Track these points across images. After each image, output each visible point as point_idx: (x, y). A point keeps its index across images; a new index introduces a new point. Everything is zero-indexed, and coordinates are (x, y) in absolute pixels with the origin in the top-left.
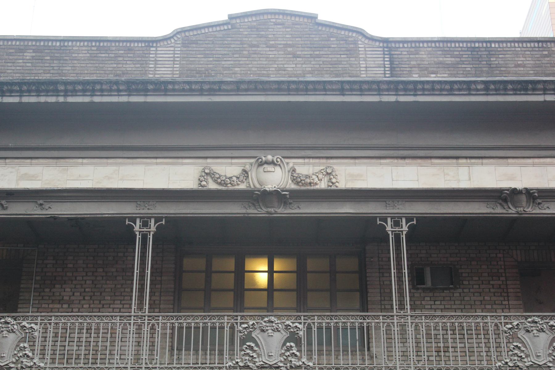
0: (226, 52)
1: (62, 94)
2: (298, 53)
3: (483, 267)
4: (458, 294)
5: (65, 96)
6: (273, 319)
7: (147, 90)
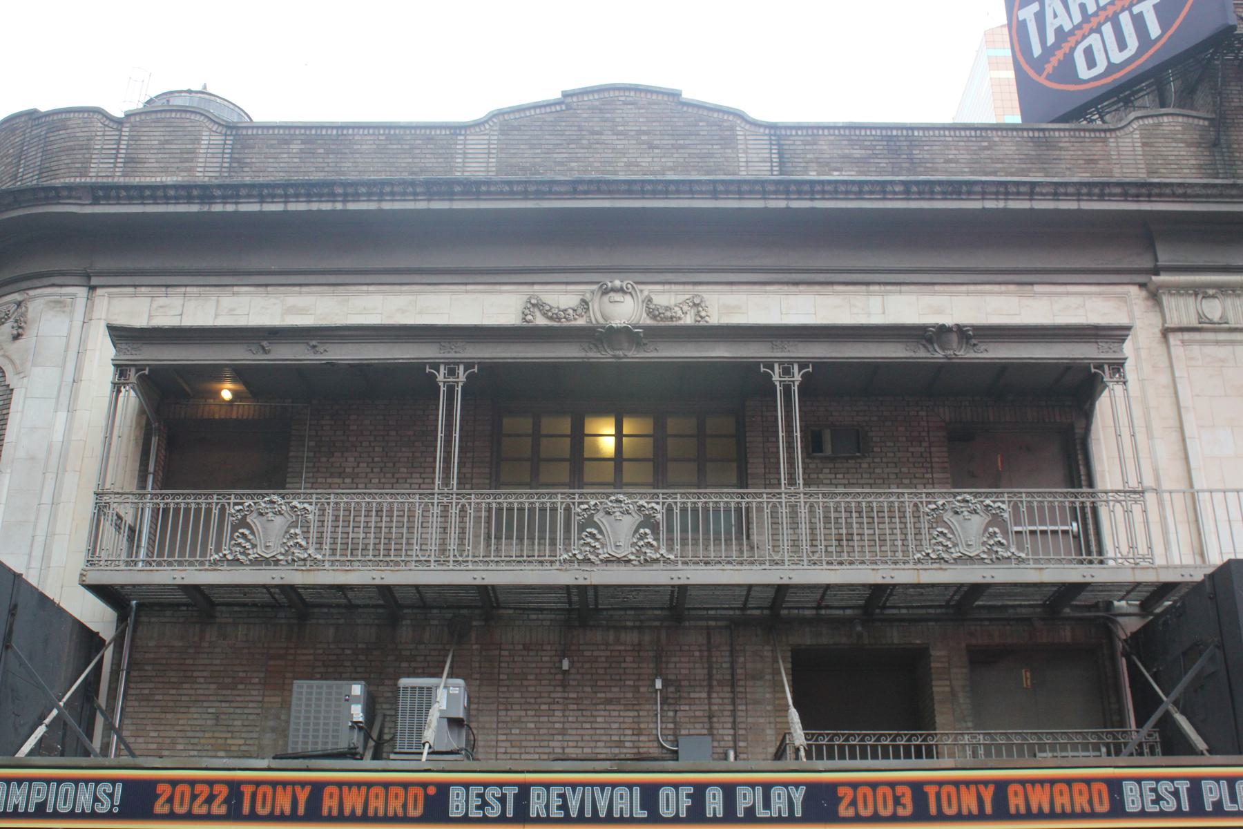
5: (345, 201)
6: (621, 497)
7: (453, 193)
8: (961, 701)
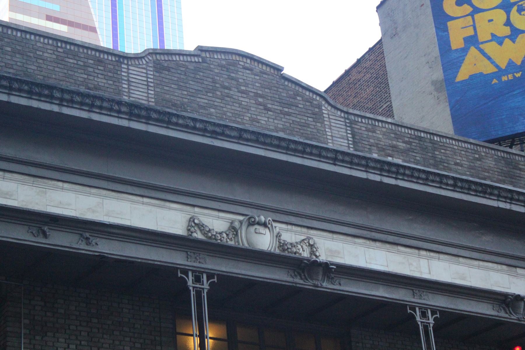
0: (199, 88)
1: (57, 102)
2: (269, 106)
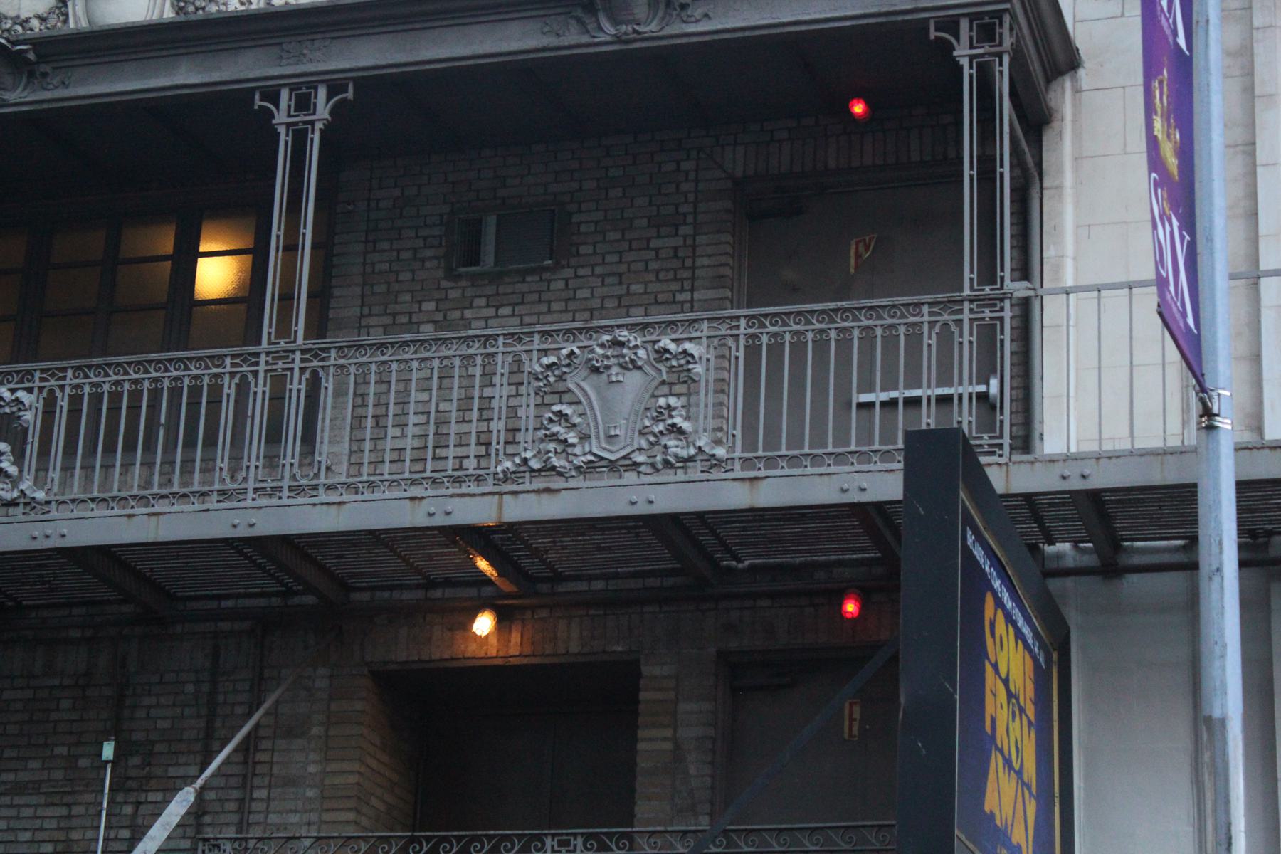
3: (639, 201)
4: (561, 284)
8: (692, 771)
